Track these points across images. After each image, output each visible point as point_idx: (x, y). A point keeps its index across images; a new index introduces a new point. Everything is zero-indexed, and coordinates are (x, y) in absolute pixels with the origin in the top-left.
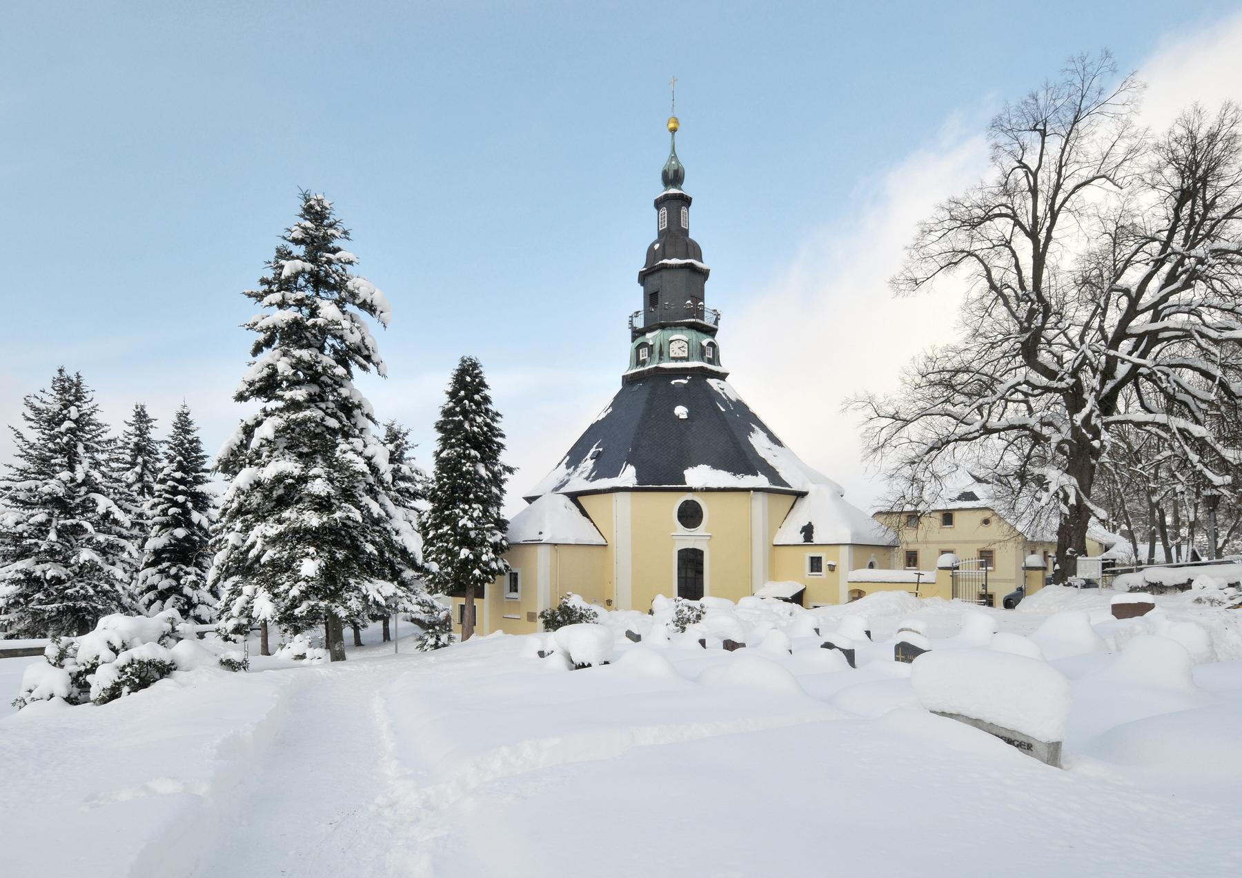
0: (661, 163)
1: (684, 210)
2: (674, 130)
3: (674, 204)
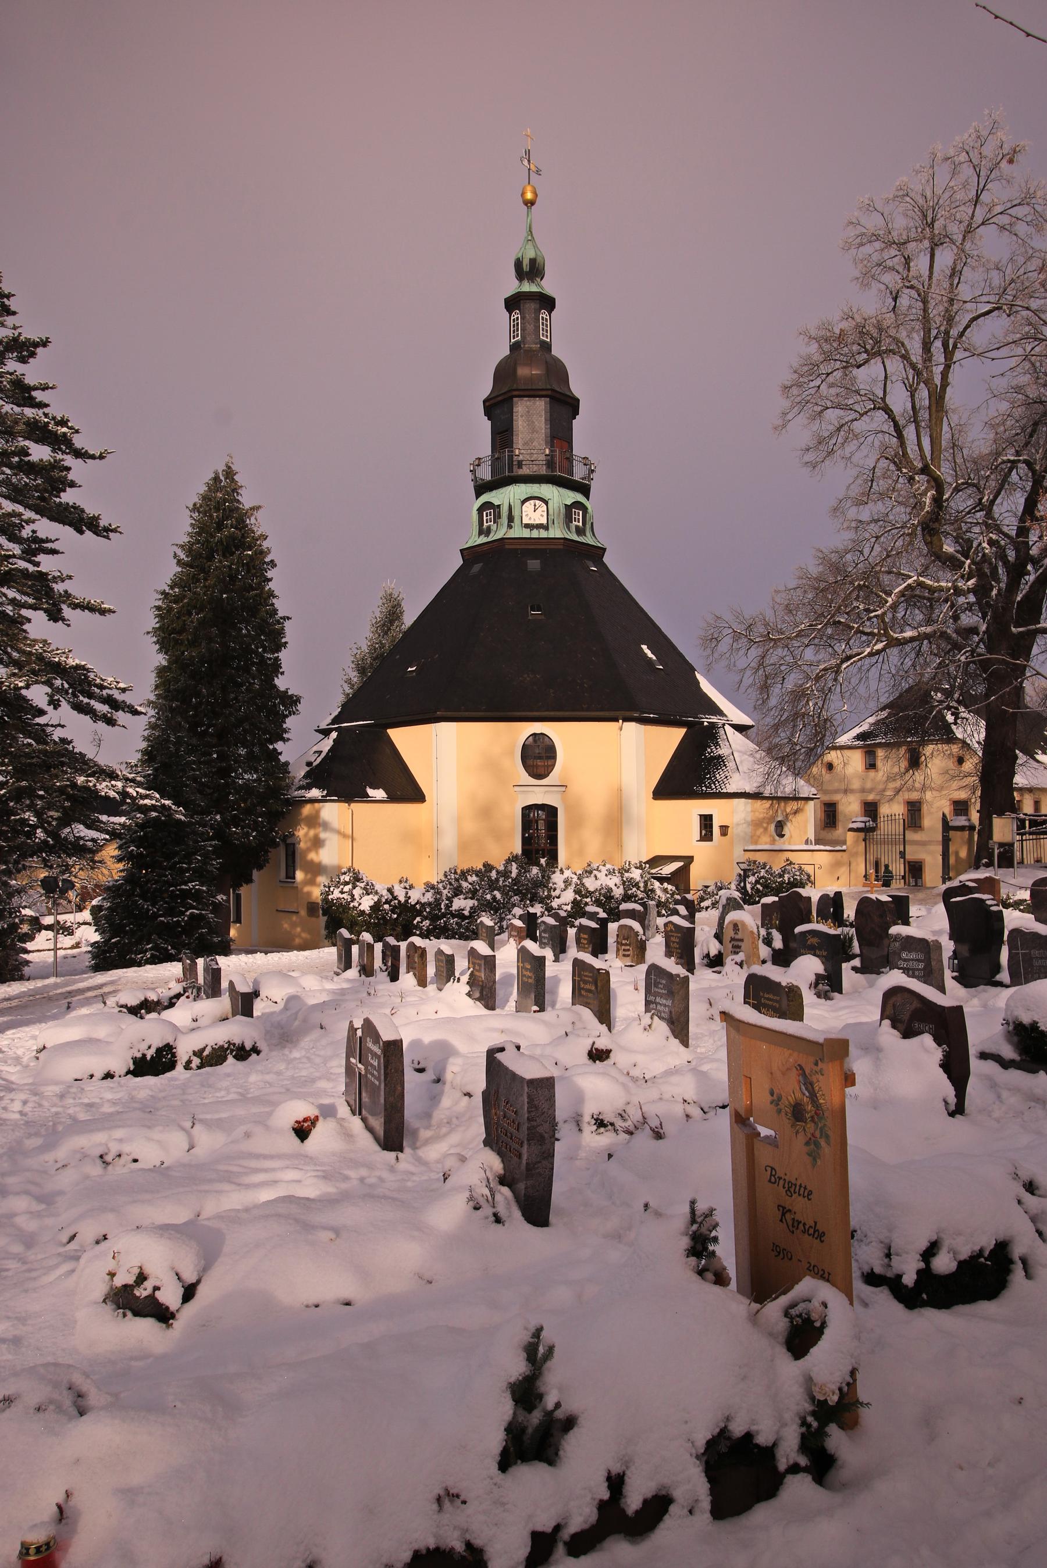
1: (544, 314)
2: (530, 204)
3: (530, 304)
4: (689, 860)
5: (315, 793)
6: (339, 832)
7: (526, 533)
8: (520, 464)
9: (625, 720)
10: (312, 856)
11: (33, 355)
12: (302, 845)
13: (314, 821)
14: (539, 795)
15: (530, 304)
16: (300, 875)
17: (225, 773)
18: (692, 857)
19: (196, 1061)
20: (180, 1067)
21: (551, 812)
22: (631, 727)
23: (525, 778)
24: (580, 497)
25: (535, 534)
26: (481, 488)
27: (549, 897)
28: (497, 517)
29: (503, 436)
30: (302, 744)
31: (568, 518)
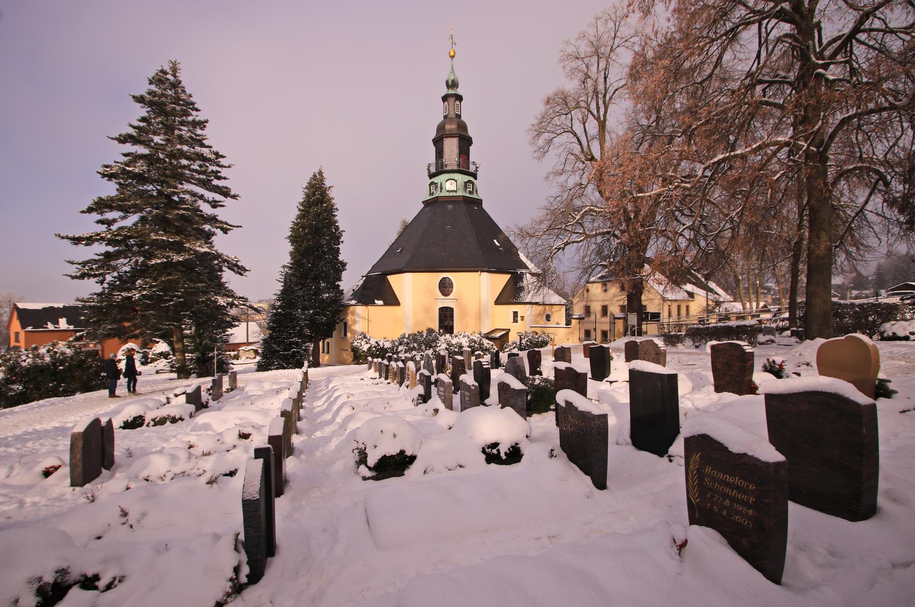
0: (447, 76)
1: (458, 102)
2: (453, 57)
3: (453, 97)
5: (353, 302)
6: (364, 318)
7: (448, 194)
8: (446, 166)
9: (482, 271)
10: (353, 327)
11: (205, 126)
12: (350, 323)
13: (353, 313)
14: (447, 302)
15: (453, 97)
16: (349, 335)
17: (316, 294)
19: (152, 423)
20: (145, 426)
22: (484, 274)
23: (440, 296)
24: (471, 179)
25: (451, 194)
26: (431, 176)
27: (436, 346)
28: (436, 187)
29: (440, 154)
30: (350, 282)
31: (466, 187)
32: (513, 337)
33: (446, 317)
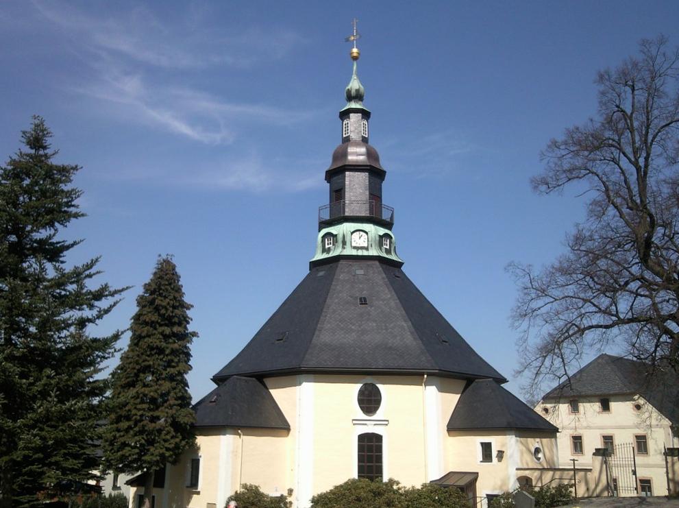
4: (475, 476)
7: (354, 252)
14: (370, 429)
18: (478, 473)
21: (378, 438)
23: (360, 415)
25: (360, 253)
26: (324, 224)
28: (335, 242)
31: (381, 245)
32: (483, 489)
33: (370, 448)
